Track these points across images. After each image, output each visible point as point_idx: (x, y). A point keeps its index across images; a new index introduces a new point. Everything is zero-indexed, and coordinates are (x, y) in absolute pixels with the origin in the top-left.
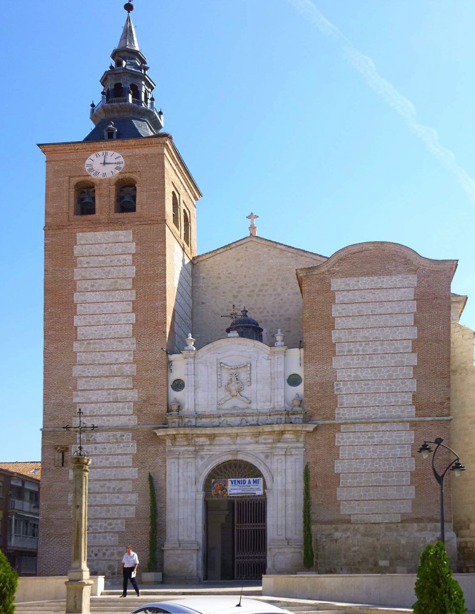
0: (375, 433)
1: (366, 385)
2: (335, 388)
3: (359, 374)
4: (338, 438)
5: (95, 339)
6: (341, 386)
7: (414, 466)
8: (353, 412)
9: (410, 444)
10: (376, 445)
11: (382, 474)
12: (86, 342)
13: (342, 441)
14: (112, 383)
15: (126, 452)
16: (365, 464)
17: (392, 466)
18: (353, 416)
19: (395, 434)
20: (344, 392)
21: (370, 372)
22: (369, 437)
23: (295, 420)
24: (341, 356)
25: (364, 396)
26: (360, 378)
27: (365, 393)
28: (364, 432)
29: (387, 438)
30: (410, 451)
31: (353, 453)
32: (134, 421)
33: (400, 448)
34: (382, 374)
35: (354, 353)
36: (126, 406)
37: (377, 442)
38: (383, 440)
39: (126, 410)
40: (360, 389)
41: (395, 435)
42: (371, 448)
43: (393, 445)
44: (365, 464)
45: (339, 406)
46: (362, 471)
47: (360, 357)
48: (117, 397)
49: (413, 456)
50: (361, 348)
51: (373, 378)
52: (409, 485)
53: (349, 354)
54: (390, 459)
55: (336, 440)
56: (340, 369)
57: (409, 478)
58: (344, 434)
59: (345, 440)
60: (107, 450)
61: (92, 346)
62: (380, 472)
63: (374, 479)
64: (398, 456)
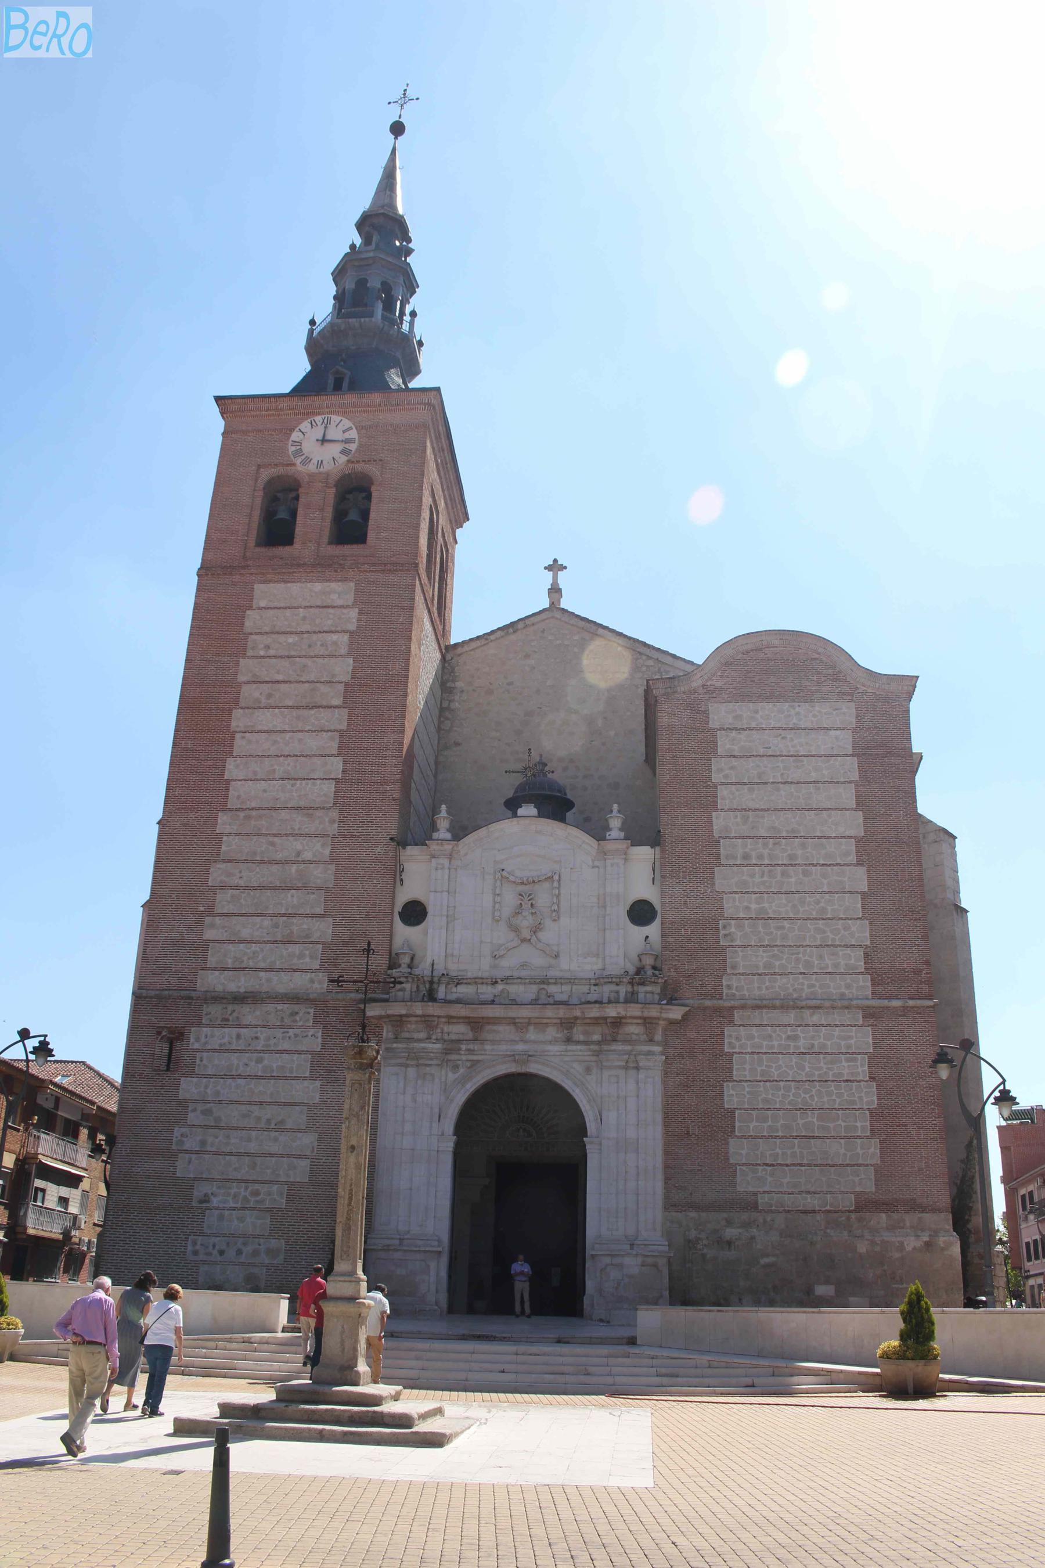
0: (799, 1029)
1: (779, 928)
2: (722, 932)
3: (766, 905)
4: (730, 1036)
5: (260, 808)
6: (733, 930)
7: (875, 1098)
8: (756, 985)
9: (866, 1053)
10: (803, 1053)
11: (816, 1112)
12: (242, 814)
13: (737, 1044)
14: (283, 902)
15: (300, 1048)
16: (782, 1092)
17: (834, 1097)
18: (757, 992)
19: (837, 1032)
20: (738, 943)
21: (784, 901)
22: (789, 1038)
23: (645, 996)
24: (730, 866)
25: (776, 952)
26: (768, 914)
27: (776, 946)
28: (779, 1025)
29: (822, 1040)
30: (866, 1068)
31: (759, 1069)
32: (320, 982)
33: (848, 1060)
34: (807, 909)
35: (754, 862)
36: (307, 952)
37: (804, 1048)
38: (816, 1043)
39: (307, 960)
40: (767, 938)
41: (836, 1033)
42: (794, 1060)
43: (835, 1054)
44: (782, 1092)
46: (778, 1106)
47: (766, 869)
48: (292, 932)
49: (872, 1079)
50: (766, 852)
51: (791, 915)
52: (867, 1137)
53: (745, 863)
54: (829, 1083)
57: (868, 1123)
58: (741, 1028)
59: (743, 1041)
60: (262, 1042)
61: (253, 823)
62: (813, 1109)
63: (801, 1122)
64: (845, 1078)
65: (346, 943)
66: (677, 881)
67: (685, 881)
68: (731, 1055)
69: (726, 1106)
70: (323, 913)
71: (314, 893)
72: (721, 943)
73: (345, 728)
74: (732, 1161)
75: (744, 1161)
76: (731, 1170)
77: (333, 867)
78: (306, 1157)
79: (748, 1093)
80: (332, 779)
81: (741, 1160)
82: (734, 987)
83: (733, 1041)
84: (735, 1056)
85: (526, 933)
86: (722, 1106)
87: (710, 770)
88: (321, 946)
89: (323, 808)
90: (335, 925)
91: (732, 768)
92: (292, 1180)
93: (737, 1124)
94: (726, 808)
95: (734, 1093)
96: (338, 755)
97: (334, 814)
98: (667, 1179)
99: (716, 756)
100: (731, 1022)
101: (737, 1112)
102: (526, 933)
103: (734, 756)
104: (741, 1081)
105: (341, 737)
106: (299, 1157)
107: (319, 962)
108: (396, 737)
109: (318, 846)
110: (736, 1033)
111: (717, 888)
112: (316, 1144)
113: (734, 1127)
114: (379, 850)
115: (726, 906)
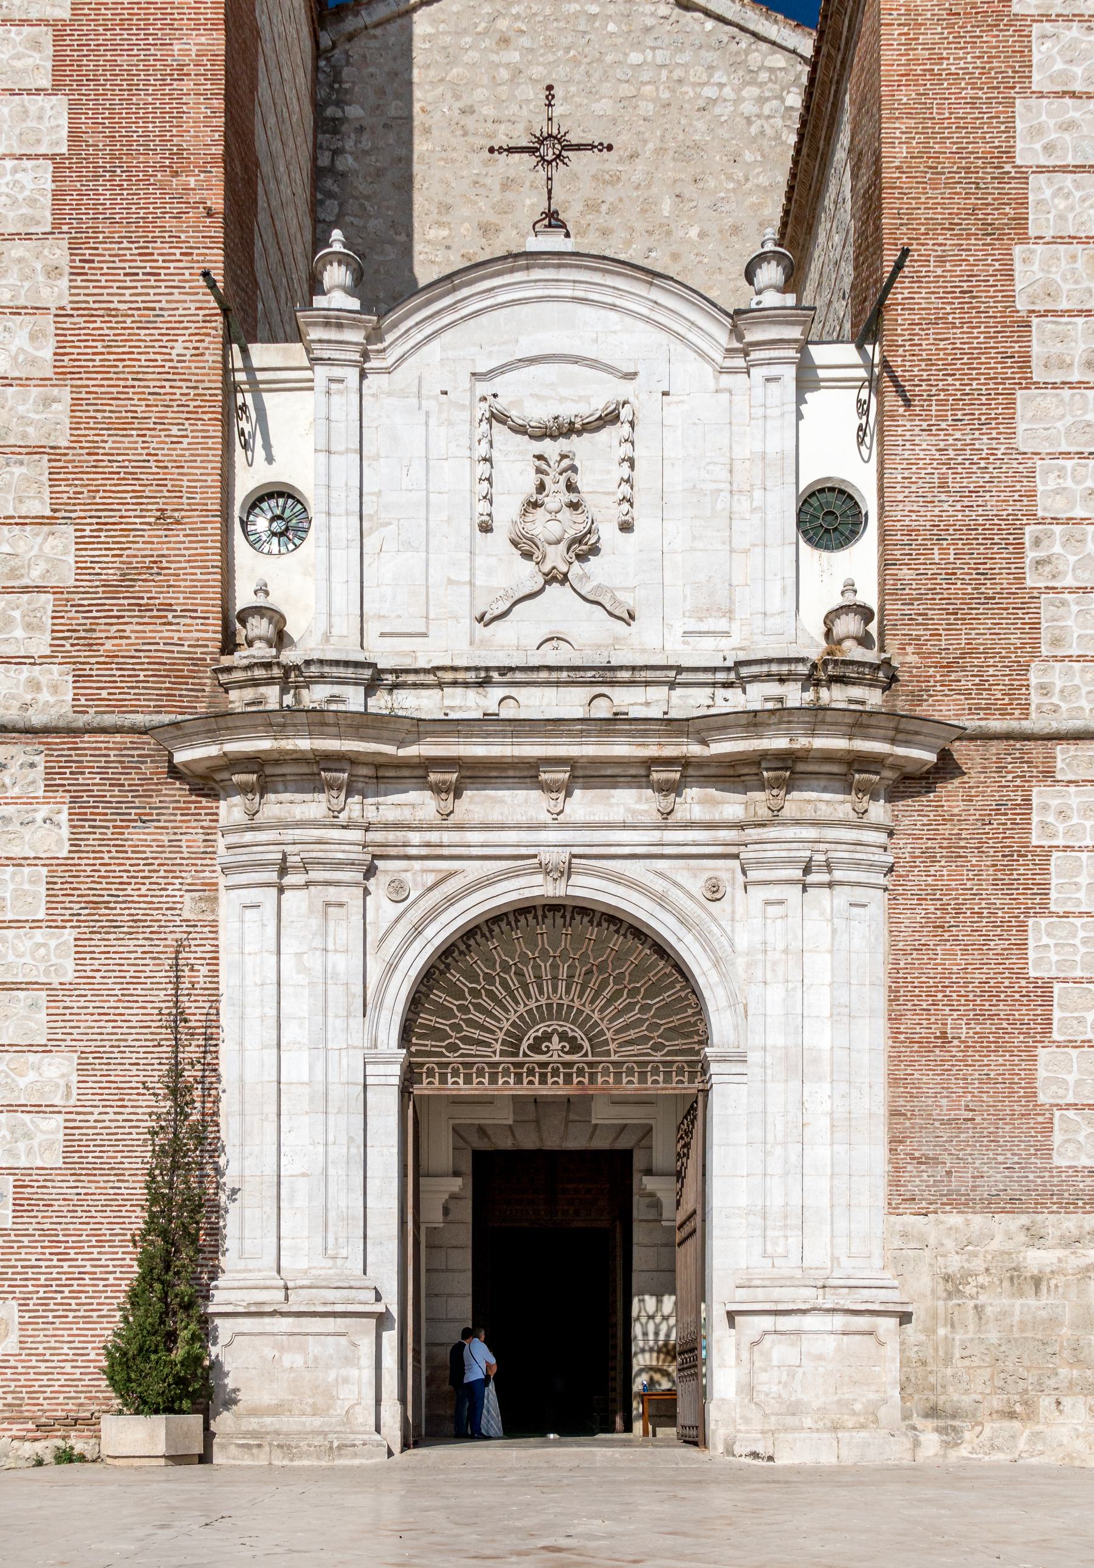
2: (1031, 555)
4: (1045, 807)
6: (1057, 549)
13: (1061, 828)
15: (16, 851)
20: (1069, 581)
24: (1054, 386)
36: (17, 614)
39: (19, 633)
45: (1045, 650)
55: (1035, 818)
56: (1054, 456)
58: (1072, 789)
59: (1075, 820)
65: (111, 589)
66: (925, 425)
67: (943, 425)
68: (1046, 852)
69: (1032, 973)
70: (48, 513)
71: (22, 463)
72: (1029, 583)
73: (66, 15)
74: (1042, 1098)
75: (1070, 1099)
76: (1040, 1119)
77: (66, 394)
78: (51, 1109)
79: (1085, 941)
80: (45, 156)
81: (1065, 1097)
82: (1057, 690)
83: (1051, 819)
84: (1055, 855)
85: (556, 558)
86: (1022, 974)
87: (1010, 131)
88: (51, 596)
89: (28, 236)
90: (80, 542)
91: (1068, 126)
92: (23, 1163)
93: (1057, 1014)
94: (1049, 234)
95: (1051, 942)
96: (55, 90)
97: (58, 253)
98: (895, 1141)
99: (1028, 92)
100: (1048, 774)
101: (1057, 987)
102: (556, 558)
103: (1073, 95)
104: (1066, 915)
105: (58, 39)
106: (37, 1109)
107: (47, 637)
108: (203, 40)
109: (20, 340)
110: (1058, 801)
111: (1022, 443)
112: (75, 1078)
113: (1049, 1021)
114: (179, 347)
115: (1040, 488)
